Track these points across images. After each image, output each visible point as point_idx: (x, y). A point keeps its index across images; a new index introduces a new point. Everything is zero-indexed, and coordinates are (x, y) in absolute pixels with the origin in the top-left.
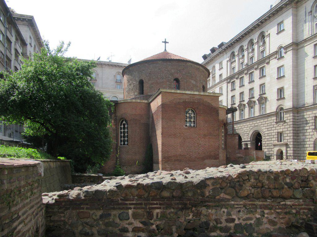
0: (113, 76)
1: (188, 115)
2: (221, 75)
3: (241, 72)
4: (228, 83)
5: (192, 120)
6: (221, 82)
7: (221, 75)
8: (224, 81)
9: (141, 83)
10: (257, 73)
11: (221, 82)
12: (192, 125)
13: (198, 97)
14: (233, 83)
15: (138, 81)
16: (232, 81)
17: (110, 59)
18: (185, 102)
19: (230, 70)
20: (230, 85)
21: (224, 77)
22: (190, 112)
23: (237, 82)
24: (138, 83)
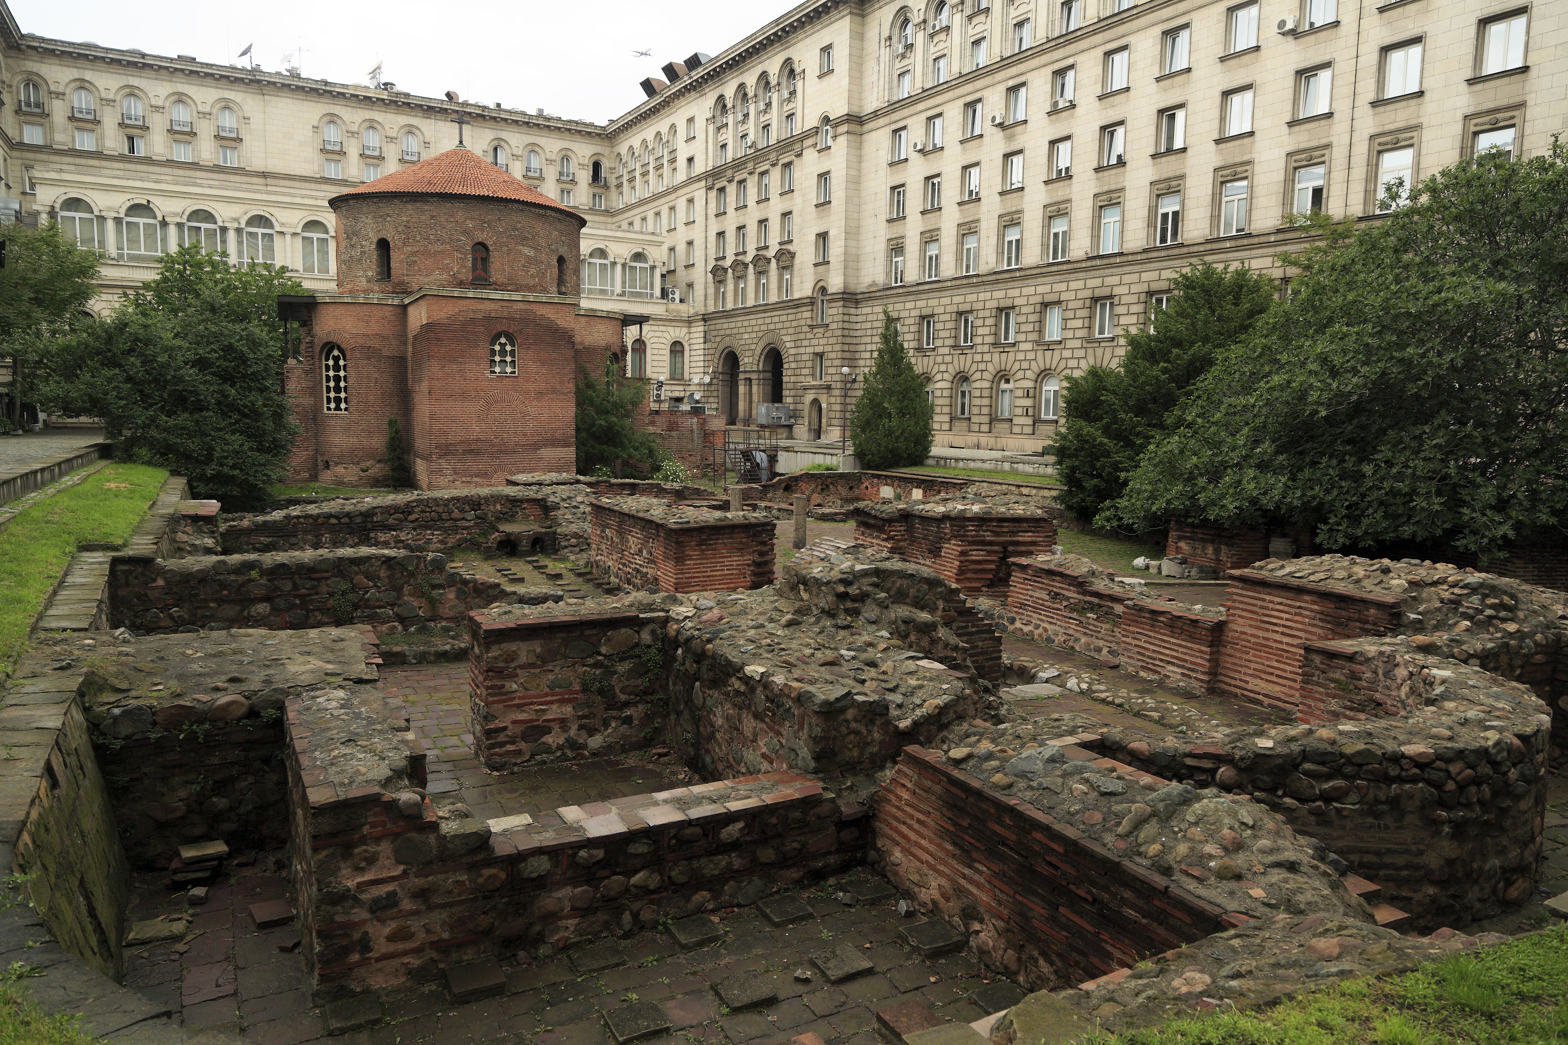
1: (497, 348)
2: (690, 160)
3: (738, 164)
4: (709, 188)
5: (509, 359)
6: (691, 181)
7: (690, 160)
8: (699, 180)
9: (383, 245)
10: (775, 177)
12: (509, 370)
13: (522, 306)
14: (722, 190)
15: (375, 240)
16: (717, 186)
17: (294, 64)
18: (488, 319)
20: (713, 194)
21: (700, 167)
22: (503, 340)
23: (732, 189)
24: (374, 246)
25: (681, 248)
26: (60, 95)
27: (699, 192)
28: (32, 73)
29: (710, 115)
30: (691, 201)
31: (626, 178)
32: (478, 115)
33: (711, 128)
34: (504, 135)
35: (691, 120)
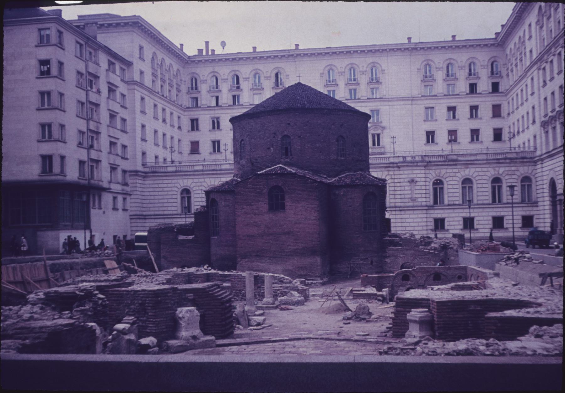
0: (319, 75)
4: (539, 69)
7: (531, 51)
11: (531, 67)
14: (544, 69)
16: (542, 67)
19: (540, 39)
20: (541, 72)
25: (530, 111)
26: (204, 81)
27: (534, 72)
28: (194, 73)
29: (536, 20)
30: (532, 79)
31: (510, 69)
32: (413, 49)
33: (538, 27)
34: (430, 57)
35: (530, 25)
